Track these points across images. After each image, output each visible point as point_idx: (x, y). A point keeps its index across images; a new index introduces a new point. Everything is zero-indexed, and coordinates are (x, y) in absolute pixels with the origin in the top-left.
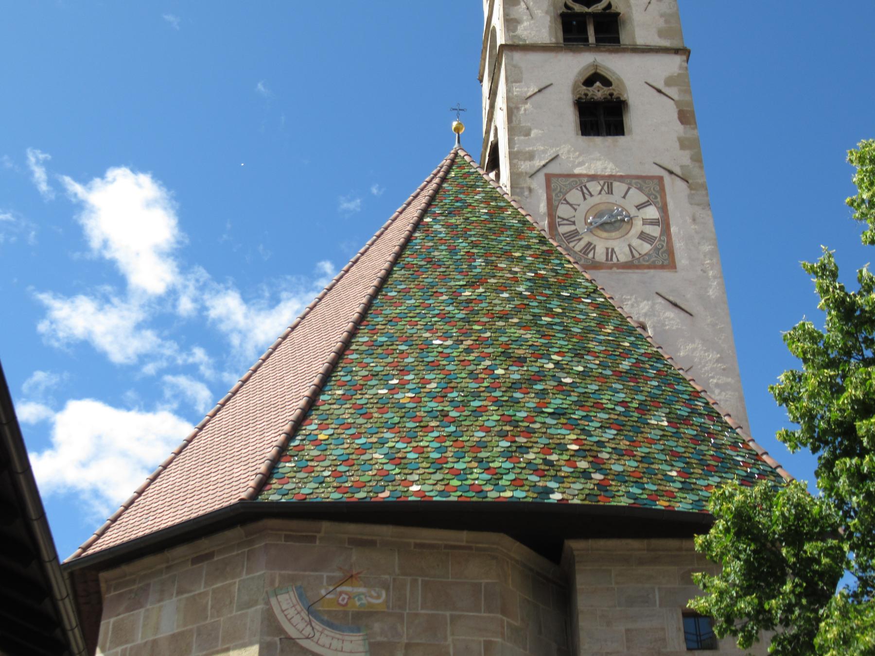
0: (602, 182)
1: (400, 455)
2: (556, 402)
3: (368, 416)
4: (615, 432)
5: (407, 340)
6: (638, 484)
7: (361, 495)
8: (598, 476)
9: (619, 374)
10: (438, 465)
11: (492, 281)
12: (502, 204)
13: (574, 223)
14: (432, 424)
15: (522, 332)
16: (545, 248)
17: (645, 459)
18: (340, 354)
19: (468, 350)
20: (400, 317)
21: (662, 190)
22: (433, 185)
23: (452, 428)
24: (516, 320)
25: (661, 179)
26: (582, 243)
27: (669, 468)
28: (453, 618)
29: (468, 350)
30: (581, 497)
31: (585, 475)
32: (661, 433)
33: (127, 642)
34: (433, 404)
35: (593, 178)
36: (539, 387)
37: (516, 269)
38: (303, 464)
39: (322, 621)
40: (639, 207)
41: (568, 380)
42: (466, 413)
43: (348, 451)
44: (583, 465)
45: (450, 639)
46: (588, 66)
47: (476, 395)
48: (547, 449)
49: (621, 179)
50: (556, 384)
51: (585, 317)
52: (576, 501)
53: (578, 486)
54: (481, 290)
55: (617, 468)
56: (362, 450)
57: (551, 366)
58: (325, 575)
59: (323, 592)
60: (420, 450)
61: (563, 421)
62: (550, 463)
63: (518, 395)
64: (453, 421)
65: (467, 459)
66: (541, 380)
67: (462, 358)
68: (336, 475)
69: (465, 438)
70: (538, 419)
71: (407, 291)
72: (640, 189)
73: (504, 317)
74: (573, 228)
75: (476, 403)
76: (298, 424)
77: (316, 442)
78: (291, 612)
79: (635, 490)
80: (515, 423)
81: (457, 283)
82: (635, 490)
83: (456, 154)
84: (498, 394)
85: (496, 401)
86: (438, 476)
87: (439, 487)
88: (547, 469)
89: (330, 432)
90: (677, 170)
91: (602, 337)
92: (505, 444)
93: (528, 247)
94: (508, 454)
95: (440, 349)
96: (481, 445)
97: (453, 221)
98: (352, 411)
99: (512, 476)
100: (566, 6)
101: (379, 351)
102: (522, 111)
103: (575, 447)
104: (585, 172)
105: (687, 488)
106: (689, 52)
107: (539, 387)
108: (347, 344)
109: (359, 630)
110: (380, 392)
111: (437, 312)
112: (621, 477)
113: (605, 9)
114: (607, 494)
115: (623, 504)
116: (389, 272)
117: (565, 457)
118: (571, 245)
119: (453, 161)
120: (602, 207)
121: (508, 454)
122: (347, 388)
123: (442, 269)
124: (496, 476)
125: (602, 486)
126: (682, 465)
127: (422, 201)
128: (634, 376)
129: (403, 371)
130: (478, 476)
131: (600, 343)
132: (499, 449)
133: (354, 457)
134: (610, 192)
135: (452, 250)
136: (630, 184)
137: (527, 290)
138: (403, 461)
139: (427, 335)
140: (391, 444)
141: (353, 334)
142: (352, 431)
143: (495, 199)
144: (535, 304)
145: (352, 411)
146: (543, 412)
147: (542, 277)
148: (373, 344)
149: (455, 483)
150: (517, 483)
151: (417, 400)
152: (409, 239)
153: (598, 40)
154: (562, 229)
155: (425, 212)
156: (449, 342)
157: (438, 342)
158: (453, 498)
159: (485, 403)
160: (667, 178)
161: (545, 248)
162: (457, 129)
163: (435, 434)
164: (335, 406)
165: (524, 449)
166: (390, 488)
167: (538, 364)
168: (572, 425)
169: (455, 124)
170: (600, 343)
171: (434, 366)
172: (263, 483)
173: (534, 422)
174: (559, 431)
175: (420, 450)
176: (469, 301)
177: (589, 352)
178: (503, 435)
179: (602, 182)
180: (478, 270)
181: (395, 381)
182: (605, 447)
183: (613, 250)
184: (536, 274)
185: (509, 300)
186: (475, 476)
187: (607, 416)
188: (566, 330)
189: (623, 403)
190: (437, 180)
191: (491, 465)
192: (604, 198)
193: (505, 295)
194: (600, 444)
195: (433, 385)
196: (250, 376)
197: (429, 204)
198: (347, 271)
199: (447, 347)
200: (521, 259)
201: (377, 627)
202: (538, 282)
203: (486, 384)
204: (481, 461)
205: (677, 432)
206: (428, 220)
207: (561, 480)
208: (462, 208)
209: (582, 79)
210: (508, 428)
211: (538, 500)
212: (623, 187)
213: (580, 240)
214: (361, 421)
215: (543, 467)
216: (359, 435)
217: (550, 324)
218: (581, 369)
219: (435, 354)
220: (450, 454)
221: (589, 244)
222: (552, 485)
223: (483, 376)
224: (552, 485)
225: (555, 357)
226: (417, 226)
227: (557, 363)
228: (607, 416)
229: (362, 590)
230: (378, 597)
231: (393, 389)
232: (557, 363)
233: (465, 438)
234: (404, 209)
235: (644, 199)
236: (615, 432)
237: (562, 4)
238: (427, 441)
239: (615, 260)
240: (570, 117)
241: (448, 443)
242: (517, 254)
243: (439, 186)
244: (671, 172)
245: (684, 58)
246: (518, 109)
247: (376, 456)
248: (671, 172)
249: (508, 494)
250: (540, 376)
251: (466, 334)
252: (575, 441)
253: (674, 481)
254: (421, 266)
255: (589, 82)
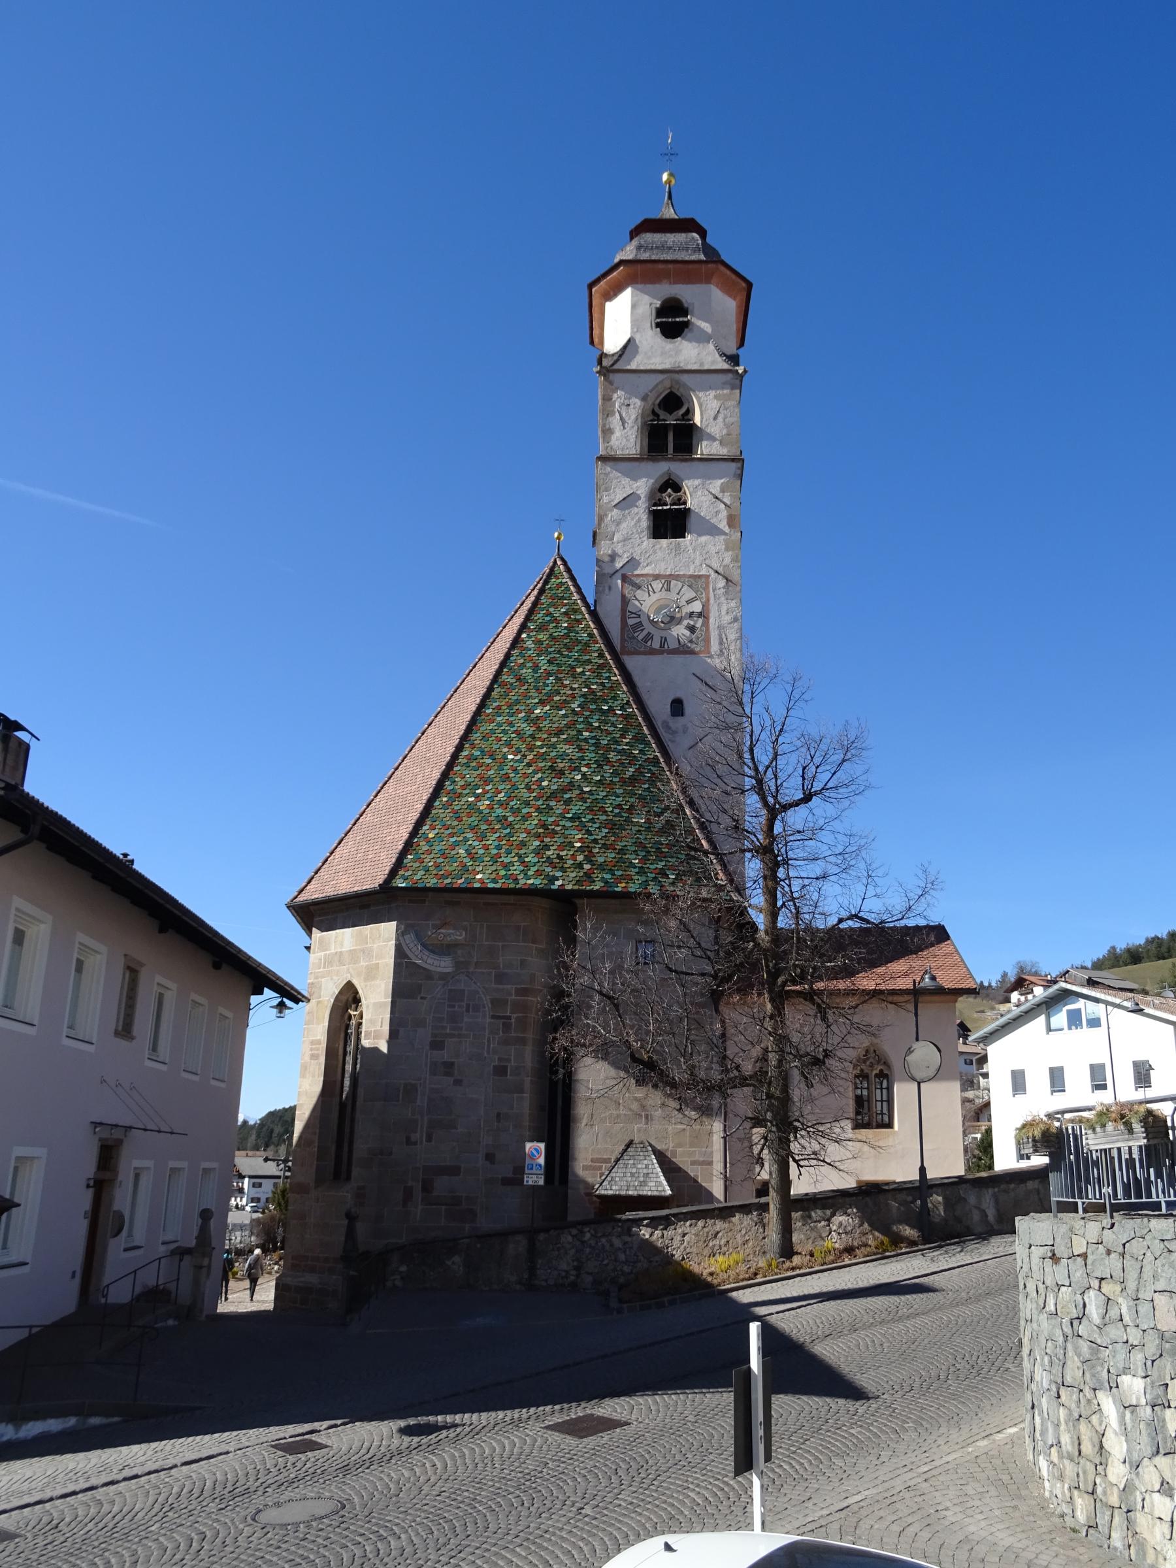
0: (663, 581)
1: (473, 851)
2: (575, 808)
3: (459, 819)
4: (607, 831)
5: (492, 755)
6: (611, 871)
7: (448, 881)
8: (587, 867)
9: (622, 780)
10: (495, 859)
11: (557, 698)
12: (578, 617)
13: (639, 616)
14: (496, 827)
15: (567, 747)
16: (601, 661)
17: (622, 851)
18: (450, 766)
19: (529, 765)
20: (493, 732)
21: (706, 588)
22: (532, 598)
23: (508, 831)
24: (565, 736)
25: (708, 577)
26: (645, 633)
27: (634, 856)
28: (503, 946)
29: (529, 765)
30: (574, 882)
31: (580, 866)
32: (637, 828)
33: (326, 950)
34: (500, 810)
35: (657, 577)
36: (567, 796)
37: (575, 686)
38: (417, 856)
39: (428, 950)
40: (689, 602)
41: (587, 789)
42: (519, 818)
43: (444, 847)
44: (580, 858)
45: (501, 958)
46: (661, 476)
47: (527, 804)
48: (561, 848)
49: (677, 577)
50: (578, 792)
51: (613, 729)
52: (569, 887)
53: (574, 874)
54: (548, 708)
55: (601, 860)
56: (454, 846)
57: (579, 777)
58: (431, 923)
59: (430, 933)
60: (486, 847)
61: (577, 823)
62: (559, 857)
63: (552, 803)
64: (510, 825)
65: (513, 855)
66: (570, 790)
67: (523, 771)
68: (437, 866)
69: (514, 838)
70: (561, 823)
71: (499, 708)
72: (690, 586)
73: (559, 732)
74: (638, 620)
75: (525, 811)
76: (419, 824)
77: (428, 840)
78: (412, 945)
79: (607, 876)
80: (544, 826)
81: (533, 701)
82: (607, 876)
83: (555, 562)
84: (540, 802)
85: (538, 809)
86: (494, 868)
87: (493, 876)
88: (558, 863)
89: (436, 831)
90: (721, 570)
91: (620, 747)
92: (537, 843)
93: (589, 662)
94: (538, 852)
95: (511, 764)
96: (523, 844)
97: (540, 637)
98: (451, 815)
99: (535, 869)
100: (654, 413)
101: (474, 764)
102: (609, 518)
103: (578, 845)
104: (651, 572)
105: (641, 871)
106: (743, 460)
107: (567, 796)
108: (455, 756)
109: (449, 955)
110: (470, 799)
111: (515, 729)
112: (602, 868)
113: (683, 415)
114: (591, 880)
115: (597, 887)
116: (490, 689)
117: (571, 852)
118: (636, 634)
119: (552, 569)
120: (662, 602)
121: (538, 852)
122: (450, 795)
123: (526, 687)
124: (527, 866)
125: (588, 876)
126: (643, 854)
127: (519, 619)
128: (633, 780)
129: (487, 782)
130: (517, 869)
131: (619, 752)
132: (531, 848)
133: (447, 852)
134: (669, 590)
135: (536, 667)
136: (683, 582)
137: (579, 706)
138: (476, 856)
139: (505, 750)
140: (470, 842)
141: (459, 748)
142: (450, 831)
143: (575, 611)
144: (581, 720)
145: (451, 815)
146: (565, 817)
147: (593, 692)
148: (470, 758)
149: (503, 873)
150: (538, 873)
151: (491, 807)
152: (508, 656)
153: (676, 450)
154: (631, 622)
155: (523, 627)
156: (518, 757)
157: (510, 757)
158: (498, 886)
159: (530, 810)
160: (713, 575)
161: (601, 661)
162: (559, 538)
163: (497, 835)
164: (441, 811)
165: (547, 847)
166: (466, 876)
167: (571, 776)
168: (582, 827)
169: (556, 535)
170: (619, 752)
171: (506, 778)
172: (393, 873)
173: (558, 825)
174: (572, 832)
175: (486, 847)
176: (538, 718)
177: (608, 761)
178: (538, 836)
179: (663, 581)
180: (550, 688)
181: (480, 791)
182: (598, 843)
183: (666, 639)
184: (589, 688)
185: (565, 716)
186: (515, 868)
187: (604, 818)
188: (597, 745)
189: (619, 806)
190: (535, 592)
191: (526, 859)
192: (664, 594)
193: (563, 712)
194: (595, 841)
195: (503, 794)
196: (400, 765)
197: (528, 618)
198: (468, 675)
199: (516, 761)
200: (583, 673)
201: (459, 952)
202: (590, 698)
203: (534, 794)
204: (520, 857)
205: (649, 827)
206: (524, 635)
207: (563, 869)
208: (550, 622)
209: (658, 486)
210: (541, 831)
211: (547, 887)
212: (680, 584)
213: (642, 630)
214: (456, 823)
215: (555, 861)
216: (451, 835)
217: (586, 740)
218: (598, 778)
219: (508, 767)
220: (503, 850)
221: (649, 633)
222: (559, 874)
223: (533, 787)
224: (559, 874)
225: (584, 769)
226: (516, 641)
227: (584, 775)
228: (604, 818)
229: (451, 931)
230: (461, 935)
231: (478, 797)
232: (584, 775)
233: (514, 838)
234: (512, 617)
235: (692, 594)
236: (607, 831)
237: (649, 412)
238: (492, 840)
239: (666, 647)
240: (645, 522)
241: (504, 842)
242: (579, 670)
243: (538, 598)
244: (717, 572)
245: (739, 465)
246: (606, 515)
247: (460, 851)
248: (717, 572)
249: (531, 882)
250: (571, 785)
251: (531, 749)
252: (580, 840)
253: (635, 867)
254: (511, 684)
255: (663, 488)
